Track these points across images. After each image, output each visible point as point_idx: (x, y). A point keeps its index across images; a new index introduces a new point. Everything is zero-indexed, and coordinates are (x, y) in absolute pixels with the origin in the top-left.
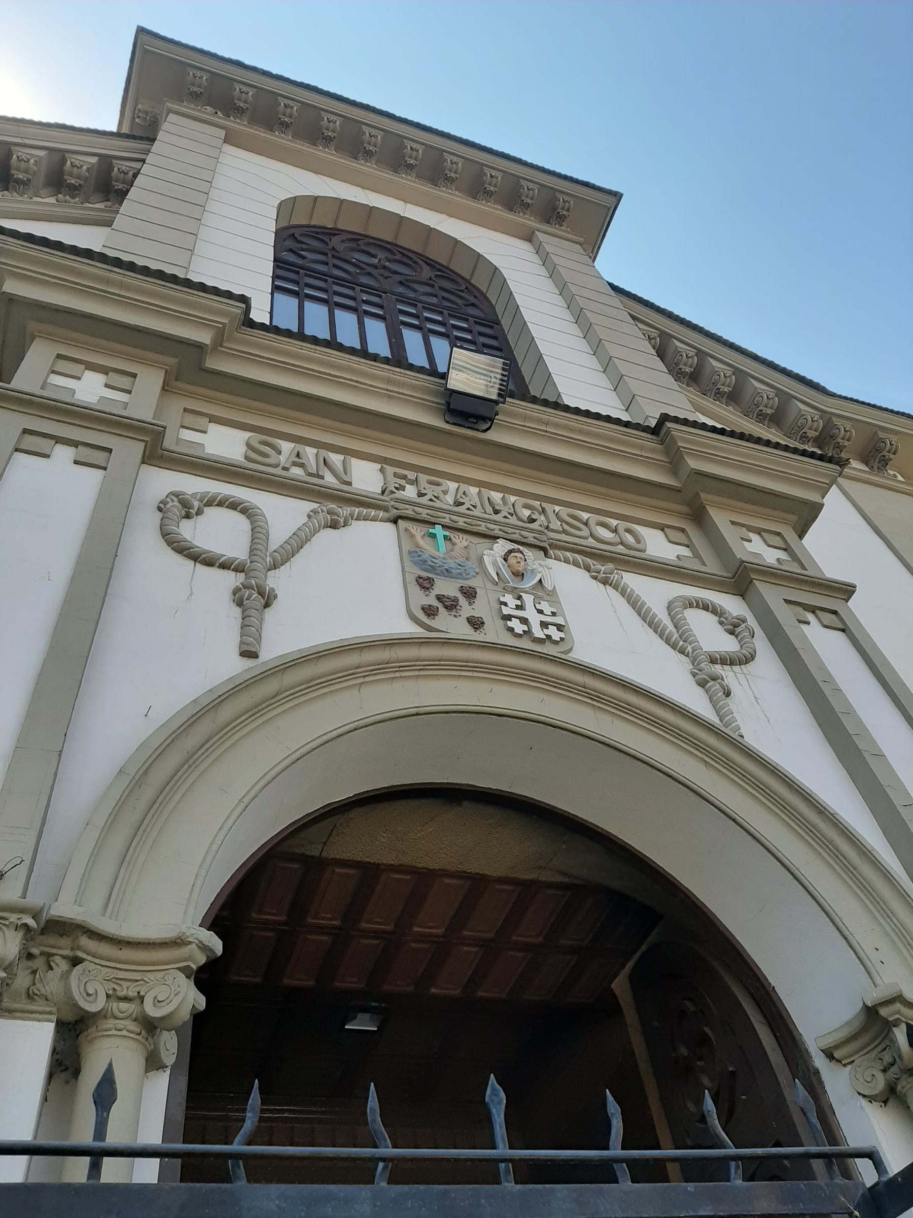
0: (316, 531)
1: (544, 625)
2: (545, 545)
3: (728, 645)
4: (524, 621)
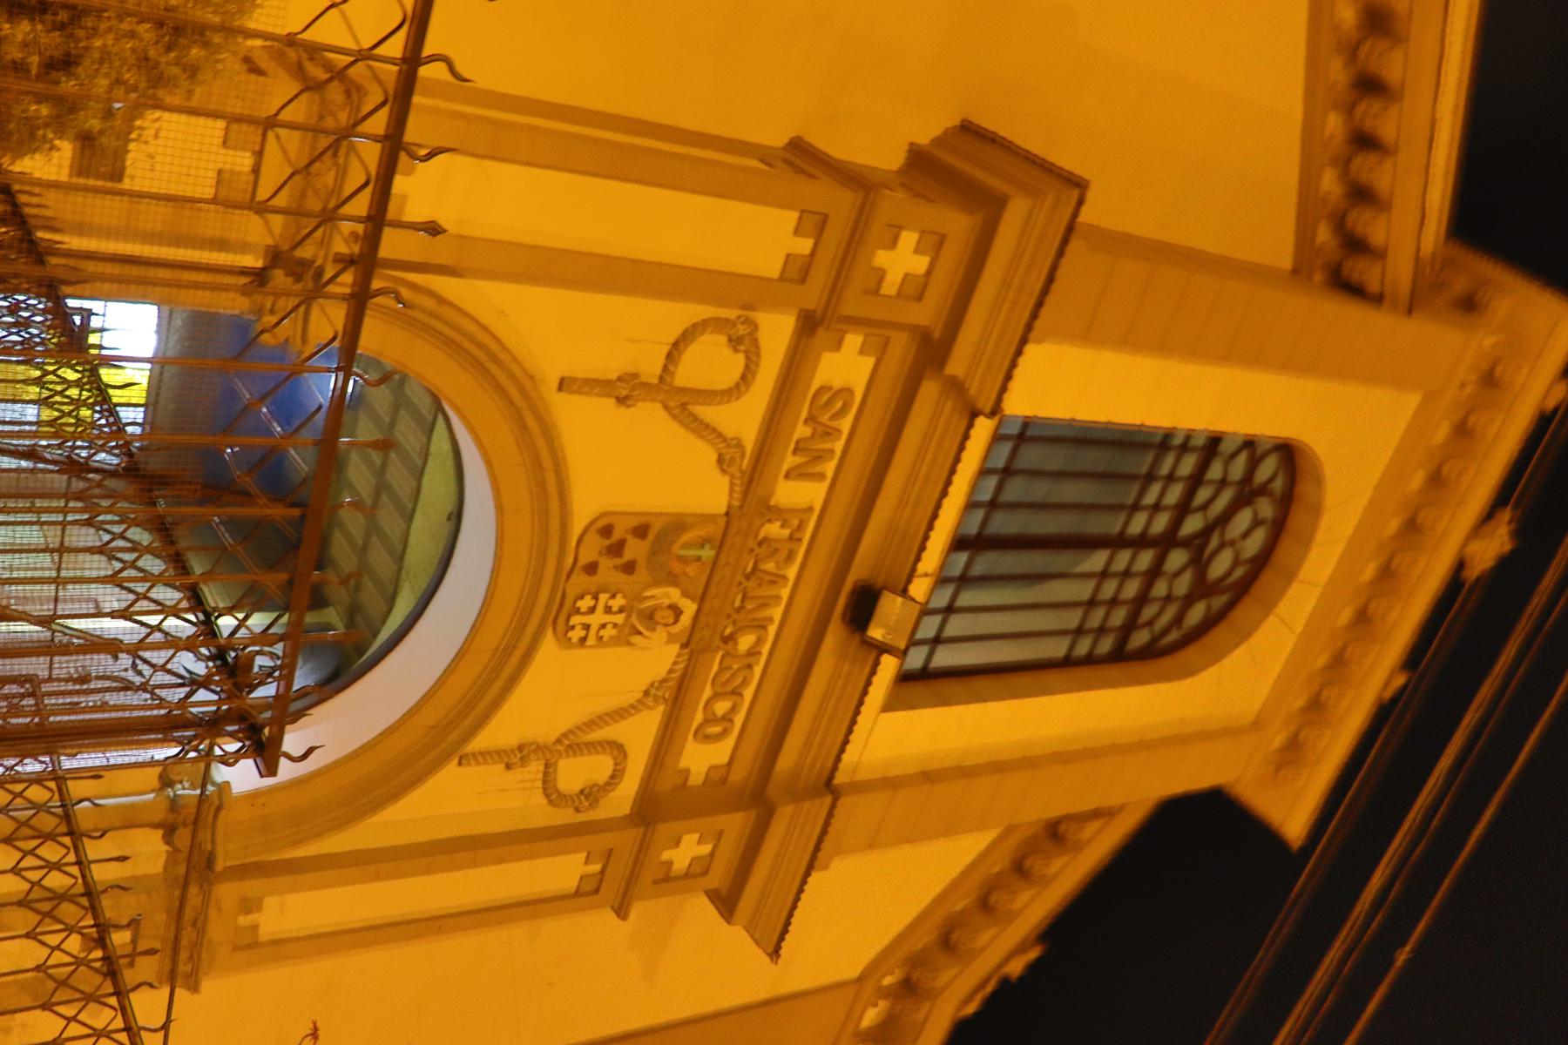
1: (587, 627)
2: (692, 646)
4: (592, 610)
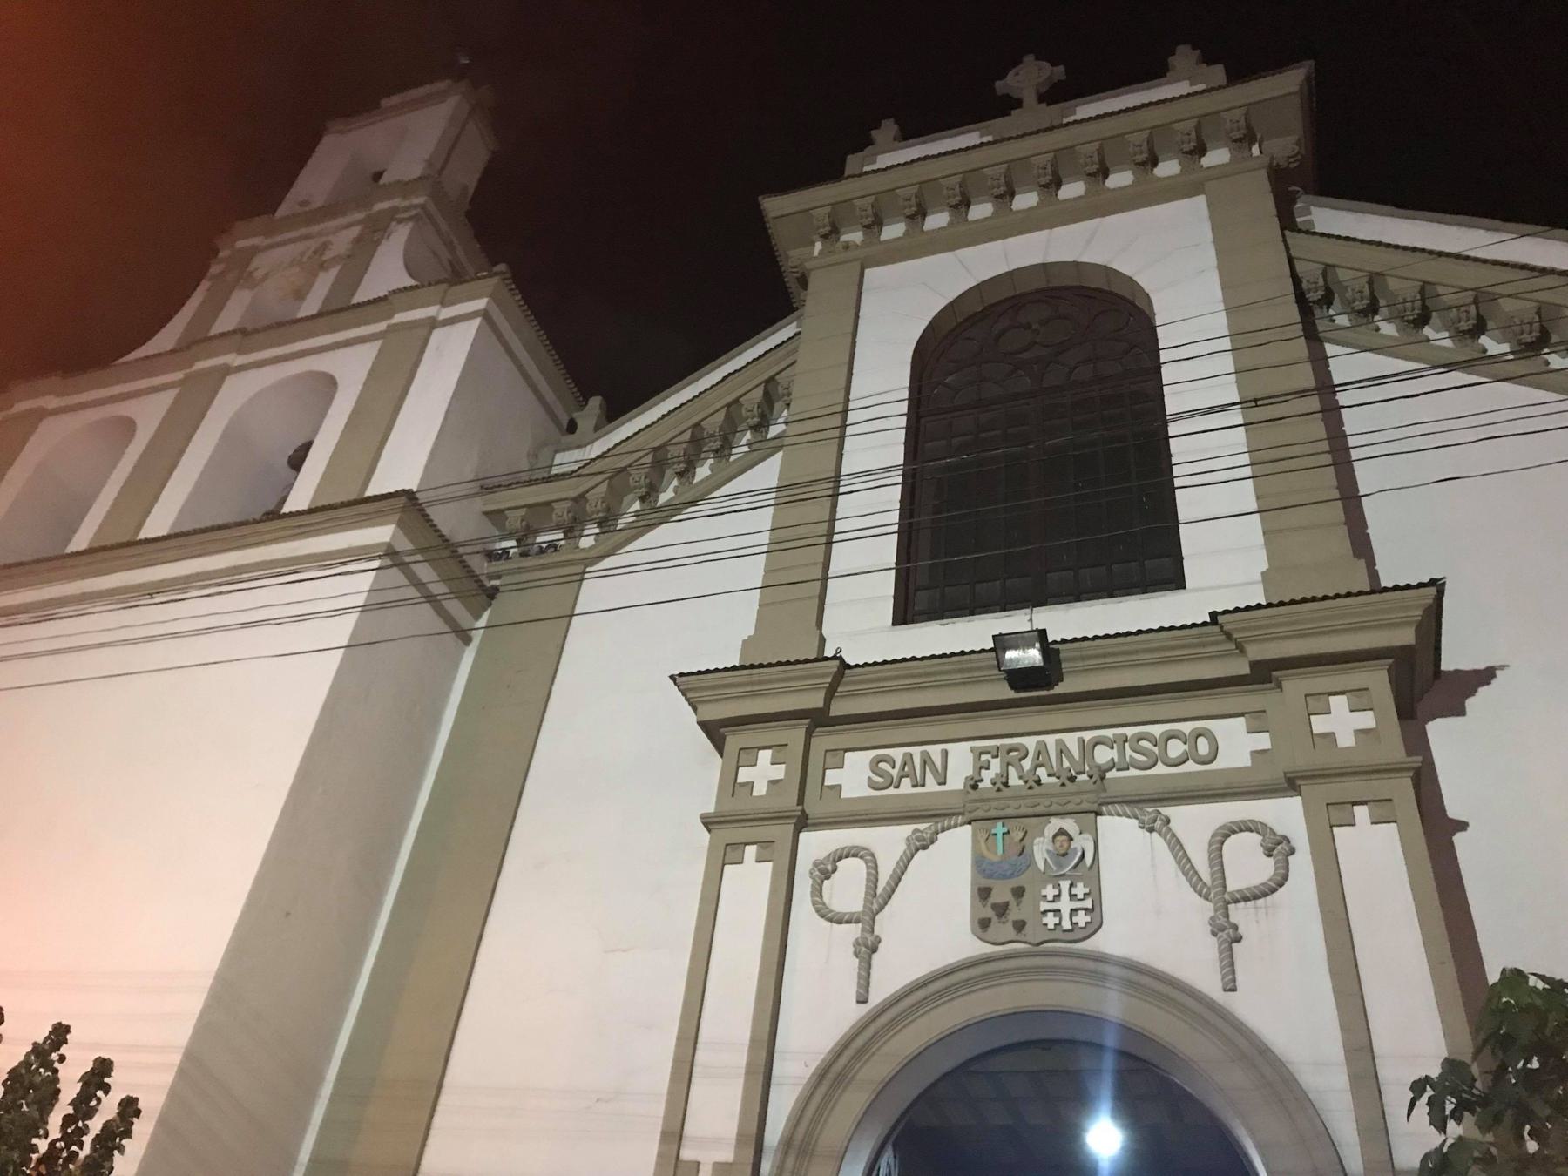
0: (912, 857)
1: (1074, 911)
2: (1095, 807)
3: (1264, 869)
4: (1057, 912)
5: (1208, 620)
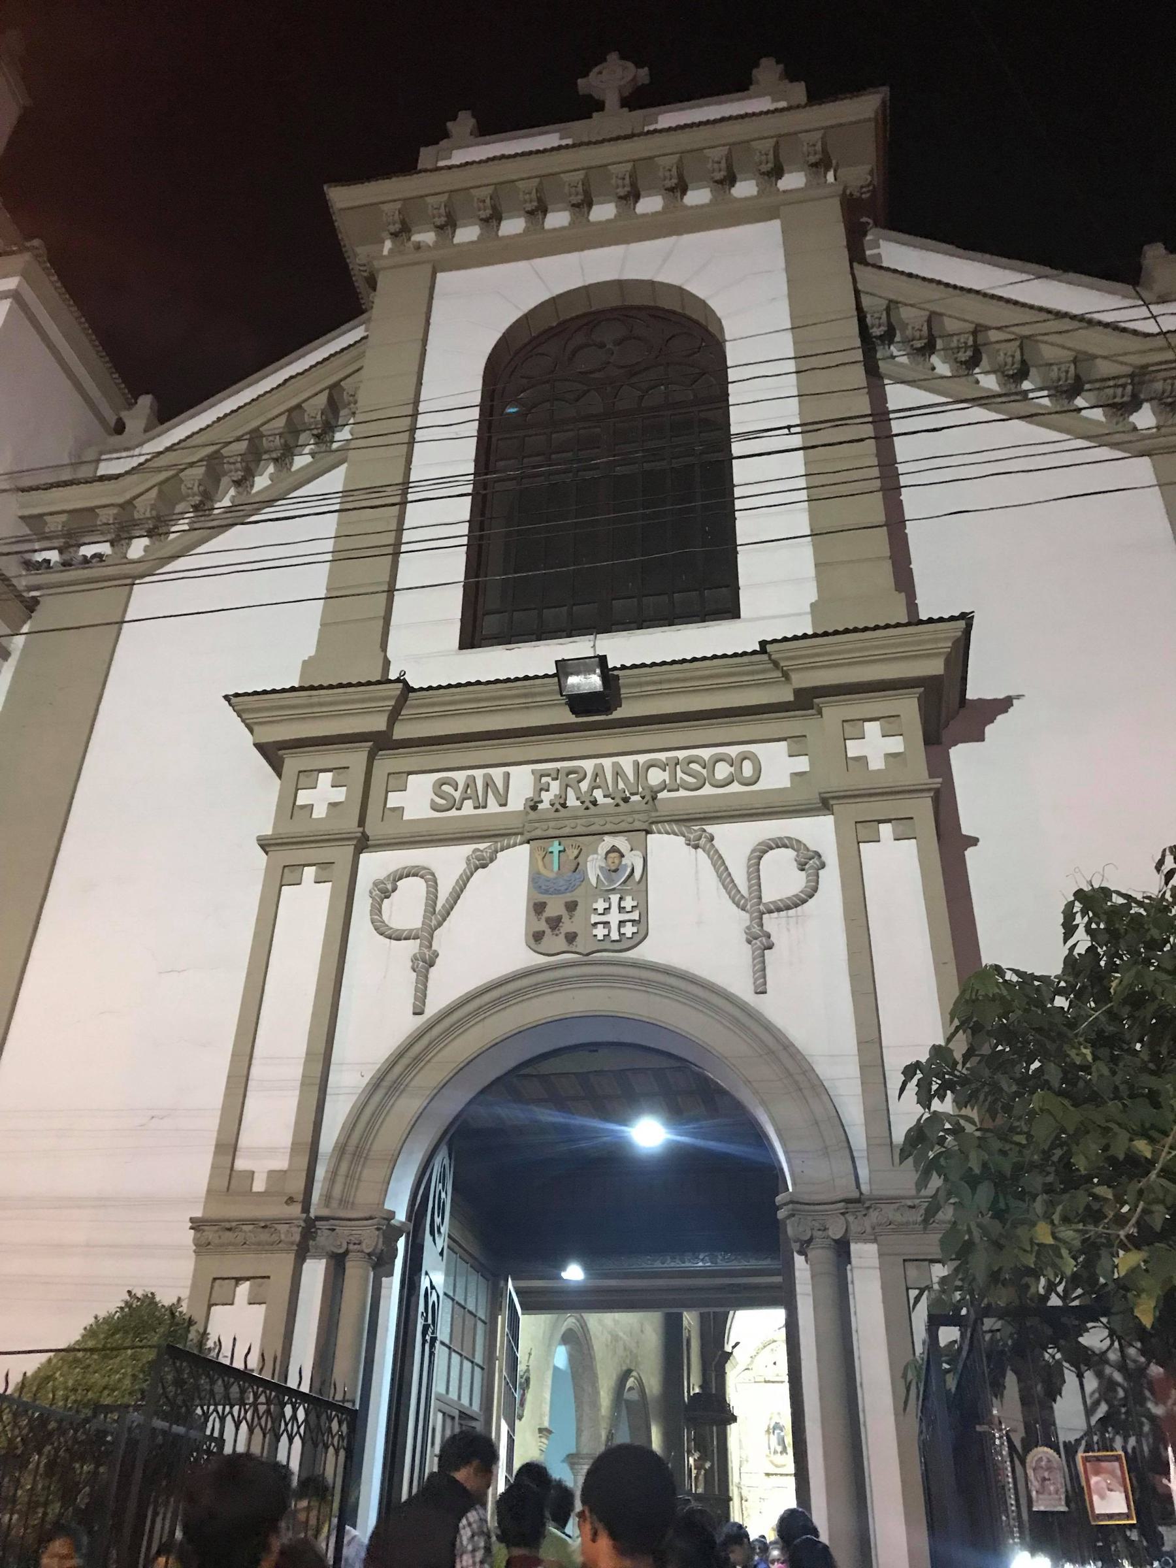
0: (472, 874)
2: (645, 826)
3: (796, 882)
4: (606, 924)
5: (758, 649)
